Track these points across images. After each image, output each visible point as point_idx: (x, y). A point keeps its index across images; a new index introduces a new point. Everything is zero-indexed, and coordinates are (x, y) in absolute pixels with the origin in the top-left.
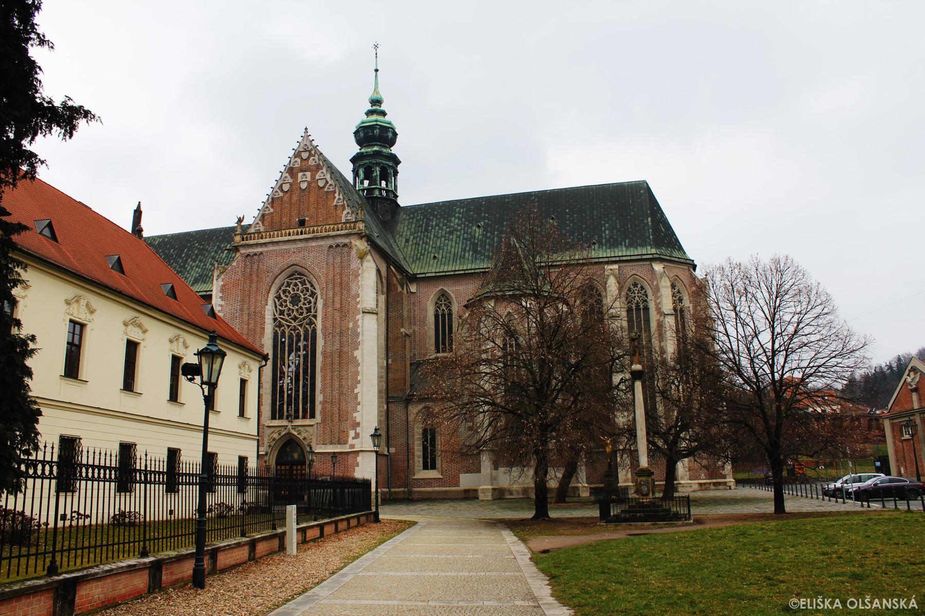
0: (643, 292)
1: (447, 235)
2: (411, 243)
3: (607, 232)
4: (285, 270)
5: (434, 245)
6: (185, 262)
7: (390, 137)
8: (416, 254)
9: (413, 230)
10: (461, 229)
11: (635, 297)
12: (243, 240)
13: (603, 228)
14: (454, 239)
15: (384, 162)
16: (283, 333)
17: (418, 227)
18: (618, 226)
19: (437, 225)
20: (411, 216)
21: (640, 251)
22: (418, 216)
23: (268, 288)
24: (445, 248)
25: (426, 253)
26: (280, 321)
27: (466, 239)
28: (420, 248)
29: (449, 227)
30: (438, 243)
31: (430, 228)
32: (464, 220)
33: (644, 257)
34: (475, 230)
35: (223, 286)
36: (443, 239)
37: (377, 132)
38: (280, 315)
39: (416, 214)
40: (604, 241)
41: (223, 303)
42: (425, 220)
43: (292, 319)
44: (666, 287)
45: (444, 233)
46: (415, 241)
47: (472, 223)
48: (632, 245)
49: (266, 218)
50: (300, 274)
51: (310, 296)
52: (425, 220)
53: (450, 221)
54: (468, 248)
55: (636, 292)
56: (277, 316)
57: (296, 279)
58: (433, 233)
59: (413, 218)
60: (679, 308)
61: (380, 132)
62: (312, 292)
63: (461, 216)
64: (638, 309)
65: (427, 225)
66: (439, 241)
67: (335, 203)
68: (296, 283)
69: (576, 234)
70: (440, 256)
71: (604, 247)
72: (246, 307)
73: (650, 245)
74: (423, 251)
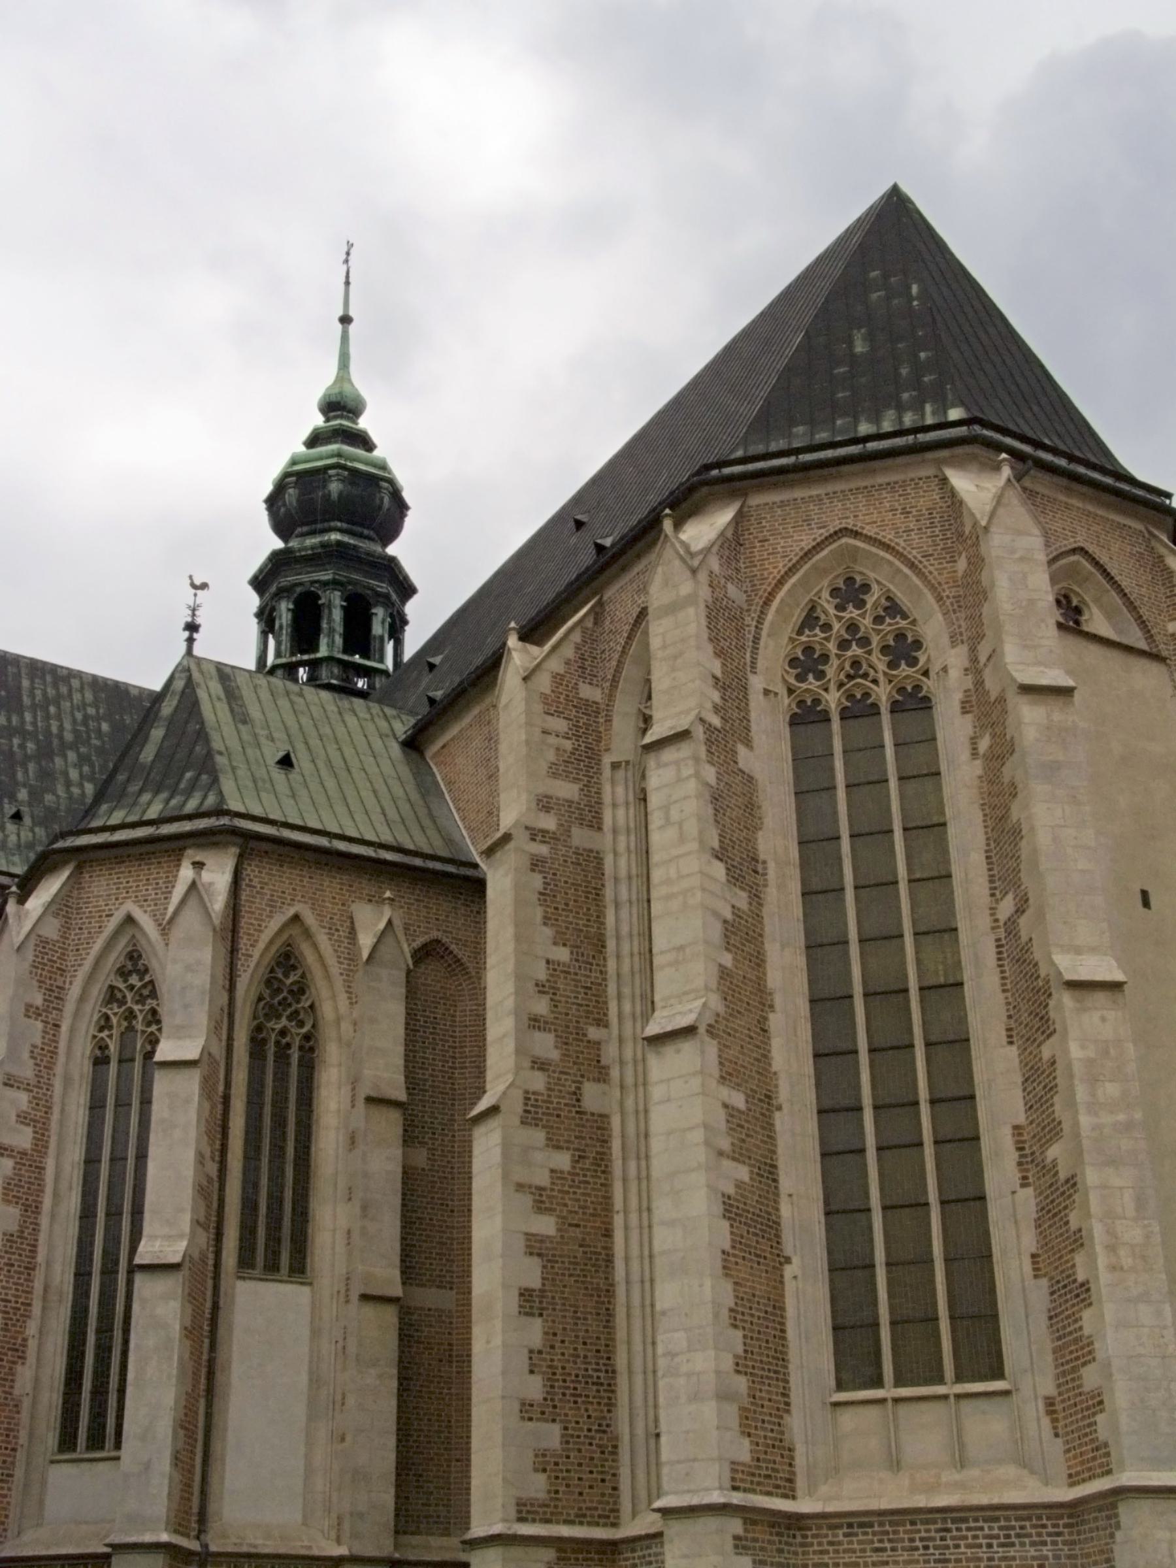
7: (334, 496)
15: (305, 578)
37: (291, 494)
44: (672, 608)
60: (883, 694)
61: (301, 494)
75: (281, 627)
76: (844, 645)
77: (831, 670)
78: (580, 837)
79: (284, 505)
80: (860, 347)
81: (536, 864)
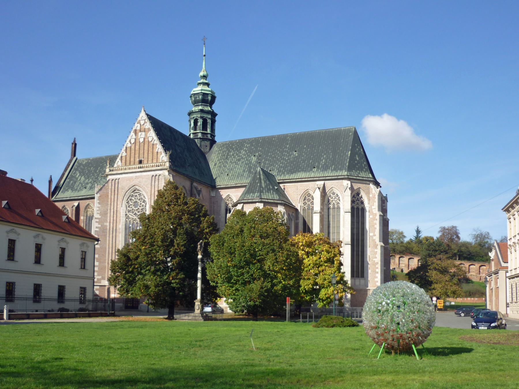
0: (337, 198)
1: (237, 161)
2: (217, 166)
3: (324, 161)
4: (131, 188)
5: (229, 168)
6: (98, 175)
8: (218, 173)
9: (220, 158)
10: (245, 158)
11: (333, 200)
12: (110, 171)
13: (322, 158)
14: (240, 164)
16: (130, 221)
17: (223, 156)
18: (331, 157)
19: (233, 155)
20: (220, 149)
21: (339, 173)
22: (224, 149)
23: (123, 198)
24: (234, 169)
25: (224, 172)
26: (128, 216)
27: (247, 164)
28: (221, 169)
29: (239, 156)
30: (231, 167)
31: (229, 157)
32: (248, 152)
33: (339, 177)
34: (252, 159)
35: (100, 196)
36: (234, 164)
38: (129, 212)
39: (223, 147)
40: (320, 166)
41: (99, 206)
42: (227, 151)
43: (134, 214)
45: (235, 160)
46: (219, 165)
47: (252, 154)
48: (335, 169)
49: (123, 158)
50: (138, 190)
51: (143, 202)
52: (227, 151)
53: (240, 153)
54: (246, 170)
55: (334, 198)
56: (127, 213)
57: (137, 193)
58: (229, 160)
59: (221, 150)
60: (360, 208)
62: (144, 200)
63: (247, 149)
64: (334, 208)
65: (228, 155)
66: (232, 165)
67: (157, 151)
68: (136, 195)
69: (306, 162)
70: (231, 175)
71: (319, 170)
72: (112, 207)
73: (345, 169)
74: (222, 171)
75: (201, 124)
76: (357, 200)
77: (356, 203)
78: (323, 213)
79: (199, 97)
80: (357, 159)
81: (320, 216)
